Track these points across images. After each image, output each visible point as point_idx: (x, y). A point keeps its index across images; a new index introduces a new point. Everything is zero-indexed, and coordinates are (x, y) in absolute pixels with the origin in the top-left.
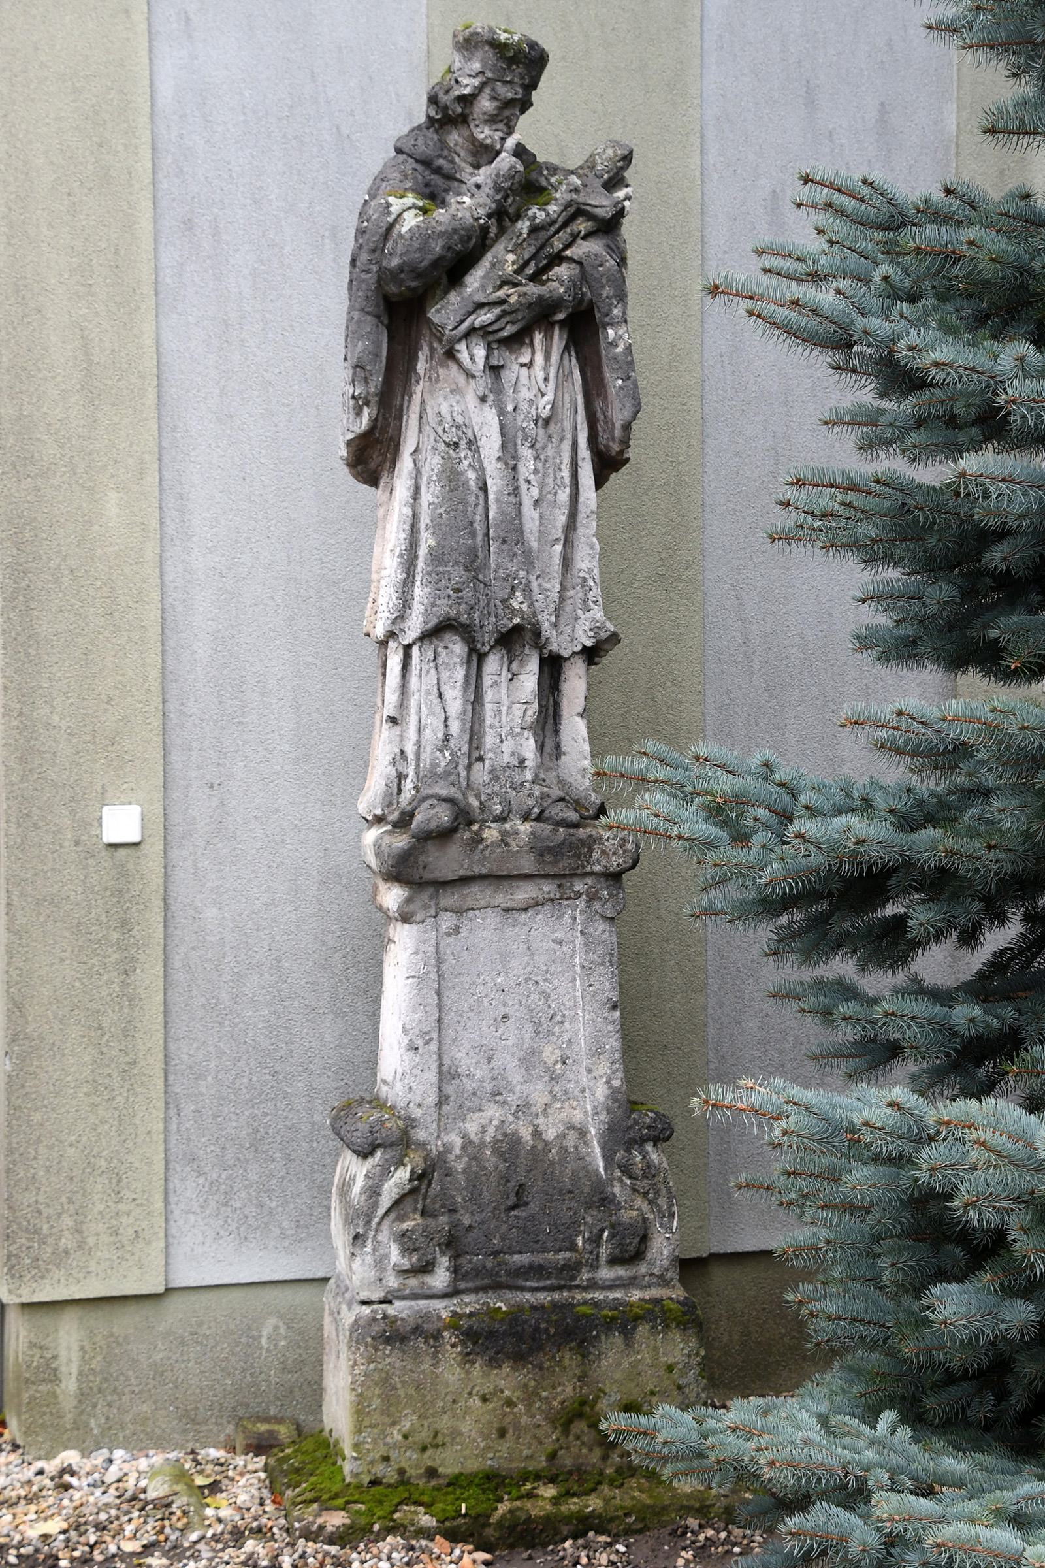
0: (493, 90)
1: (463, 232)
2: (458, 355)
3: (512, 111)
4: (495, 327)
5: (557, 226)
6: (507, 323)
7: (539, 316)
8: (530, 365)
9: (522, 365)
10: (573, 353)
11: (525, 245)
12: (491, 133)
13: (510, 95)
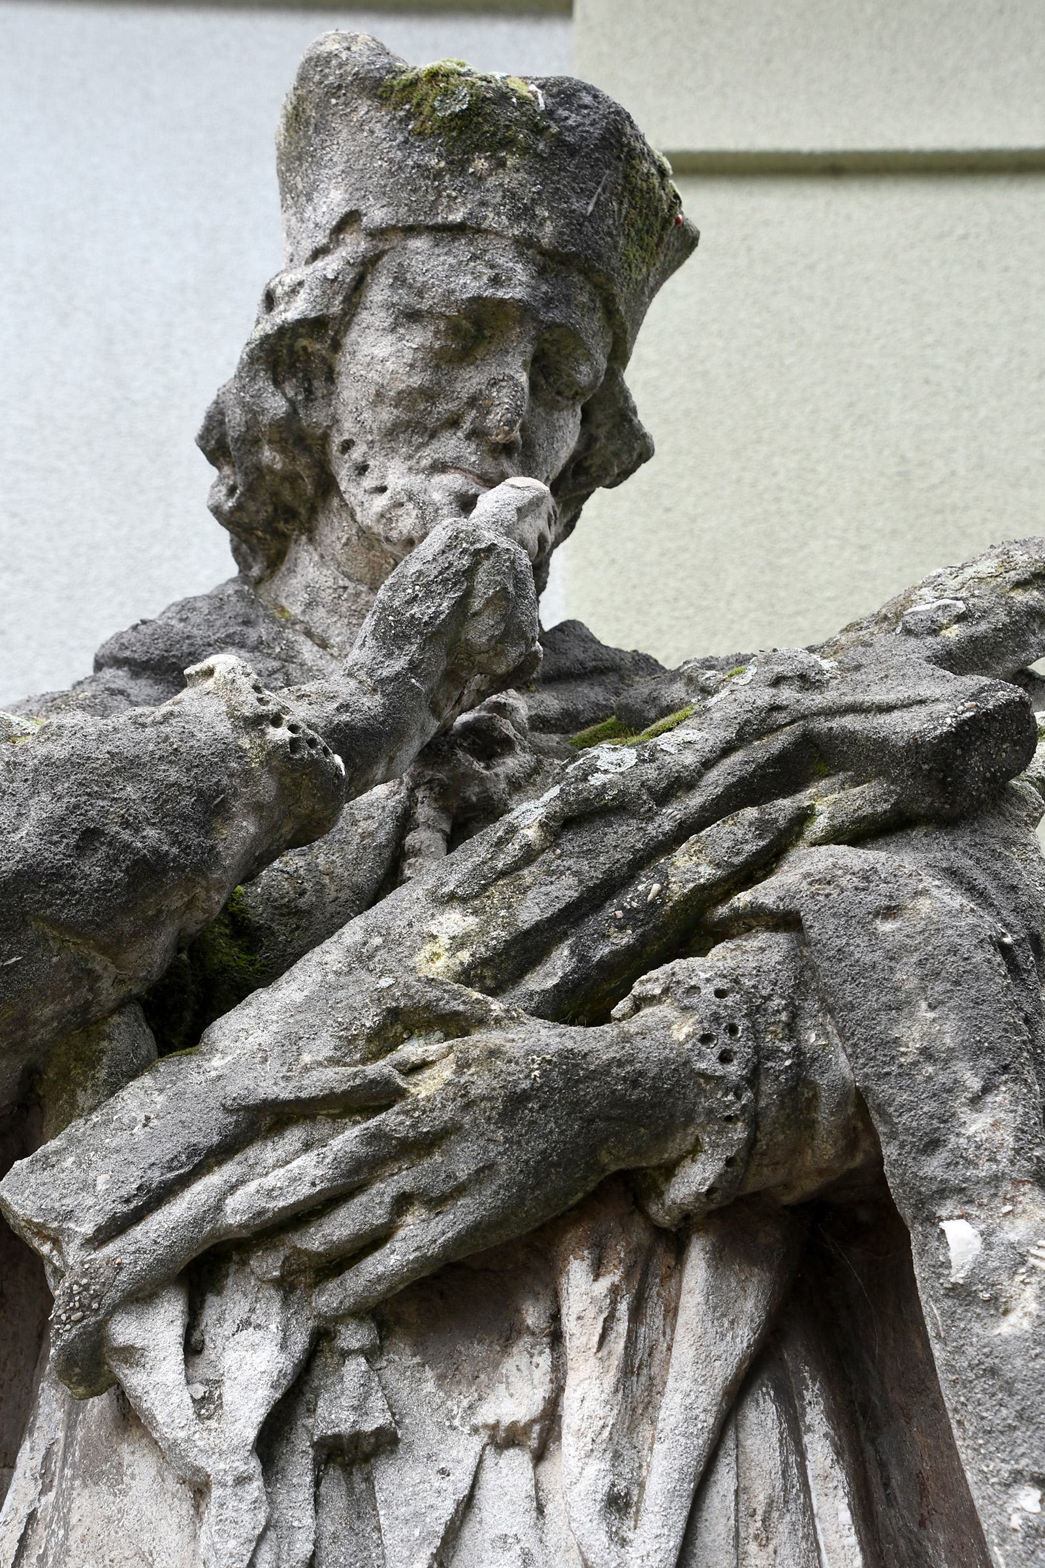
0: (400, 280)
1: (173, 775)
2: (134, 1379)
3: (494, 371)
4: (340, 1226)
5: (695, 800)
6: (402, 1203)
7: (583, 1185)
8: (541, 1436)
9: (505, 1439)
10: (815, 1416)
11: (528, 875)
12: (416, 482)
13: (470, 285)
